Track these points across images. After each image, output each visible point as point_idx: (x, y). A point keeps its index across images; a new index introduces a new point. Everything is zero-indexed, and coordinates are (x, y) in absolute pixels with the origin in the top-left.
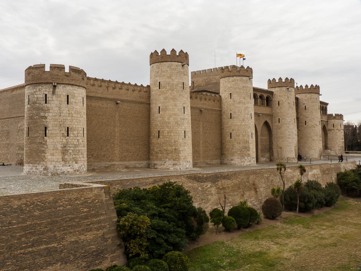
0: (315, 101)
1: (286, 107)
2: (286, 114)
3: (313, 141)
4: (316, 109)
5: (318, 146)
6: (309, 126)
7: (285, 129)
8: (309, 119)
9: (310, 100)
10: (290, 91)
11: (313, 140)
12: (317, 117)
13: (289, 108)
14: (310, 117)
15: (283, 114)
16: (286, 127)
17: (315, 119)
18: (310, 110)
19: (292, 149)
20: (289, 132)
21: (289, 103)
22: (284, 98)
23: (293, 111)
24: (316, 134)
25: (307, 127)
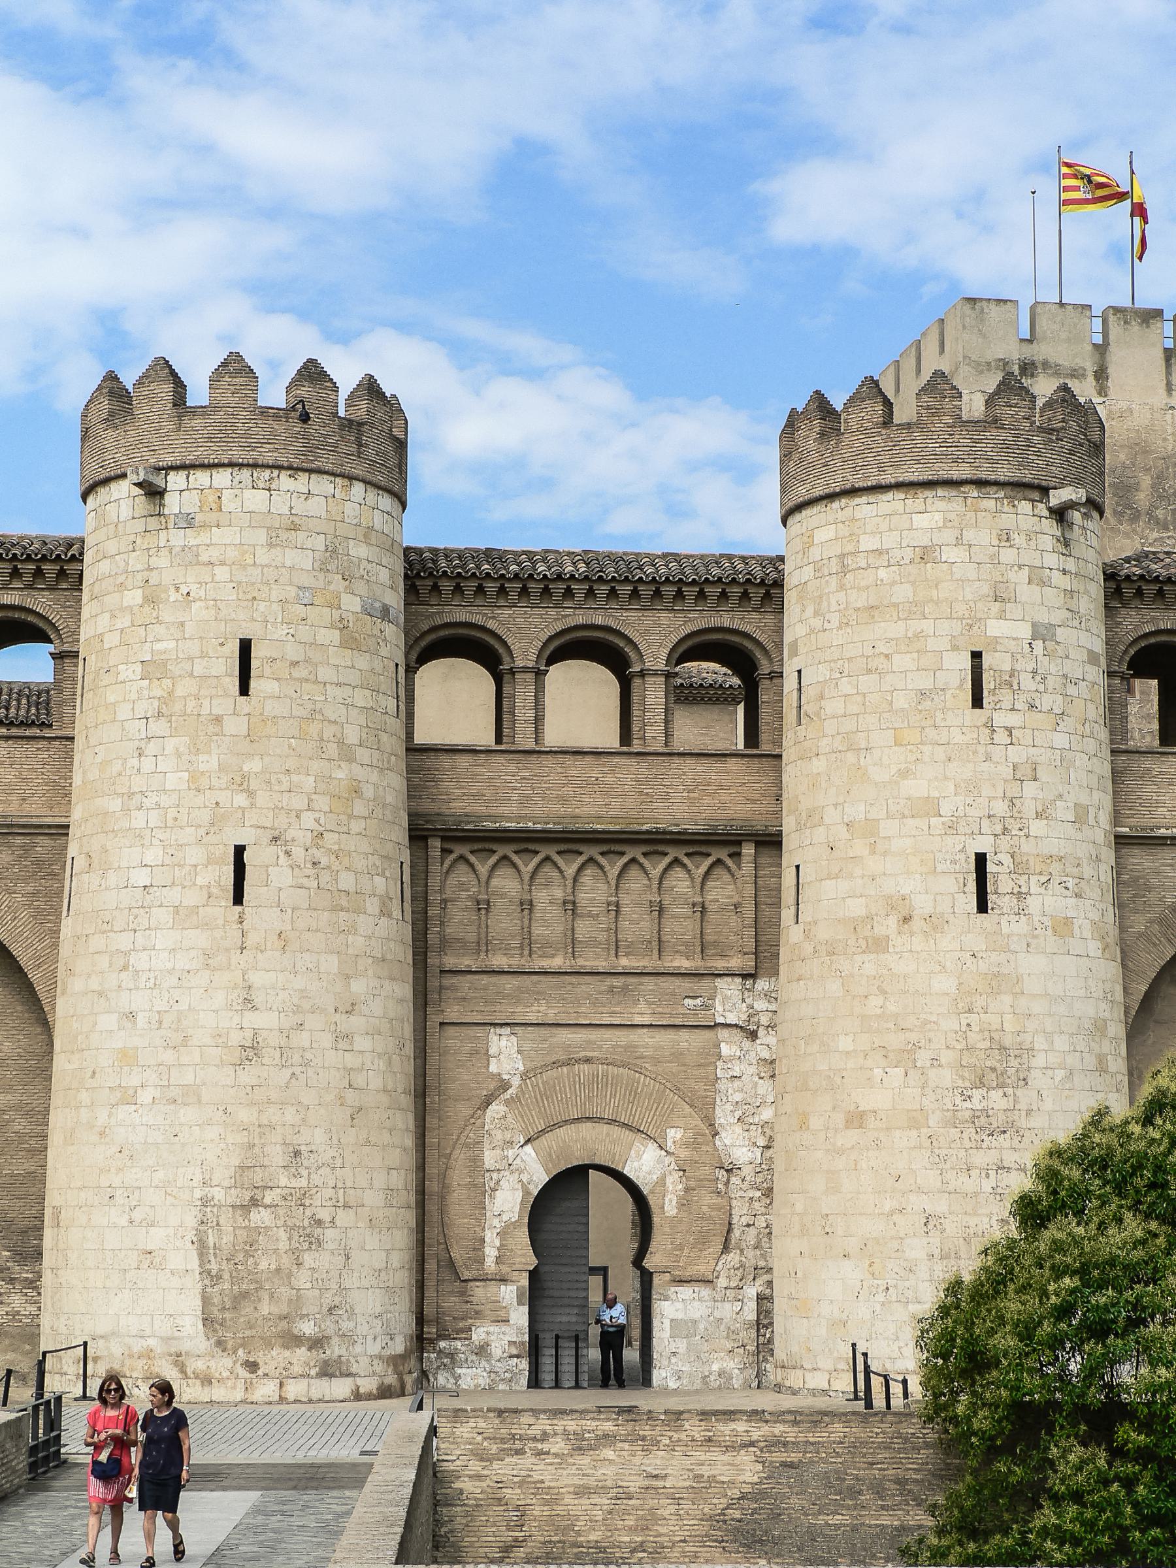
0: (904, 592)
1: (124, 712)
2: (115, 804)
3: (853, 1136)
4: (901, 702)
5: (917, 1203)
6: (823, 933)
7: (94, 984)
8: (820, 835)
9: (842, 587)
10: (189, 521)
11: (856, 1119)
12: (930, 807)
13: (158, 727)
14: (831, 815)
15: (99, 801)
16: (104, 962)
17: (888, 828)
18: (830, 727)
19: (155, 1238)
20: (132, 1016)
21: (153, 669)
22: (113, 616)
23: (208, 762)
24: (895, 1041)
25: (808, 949)
